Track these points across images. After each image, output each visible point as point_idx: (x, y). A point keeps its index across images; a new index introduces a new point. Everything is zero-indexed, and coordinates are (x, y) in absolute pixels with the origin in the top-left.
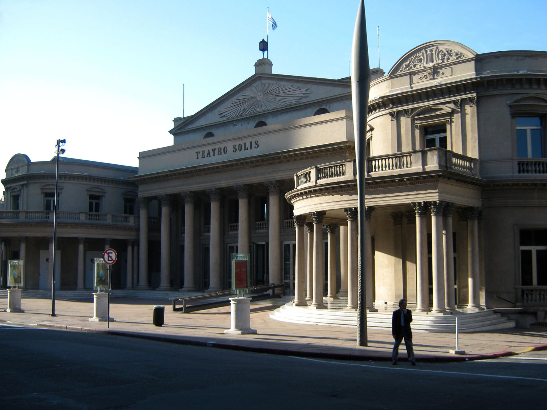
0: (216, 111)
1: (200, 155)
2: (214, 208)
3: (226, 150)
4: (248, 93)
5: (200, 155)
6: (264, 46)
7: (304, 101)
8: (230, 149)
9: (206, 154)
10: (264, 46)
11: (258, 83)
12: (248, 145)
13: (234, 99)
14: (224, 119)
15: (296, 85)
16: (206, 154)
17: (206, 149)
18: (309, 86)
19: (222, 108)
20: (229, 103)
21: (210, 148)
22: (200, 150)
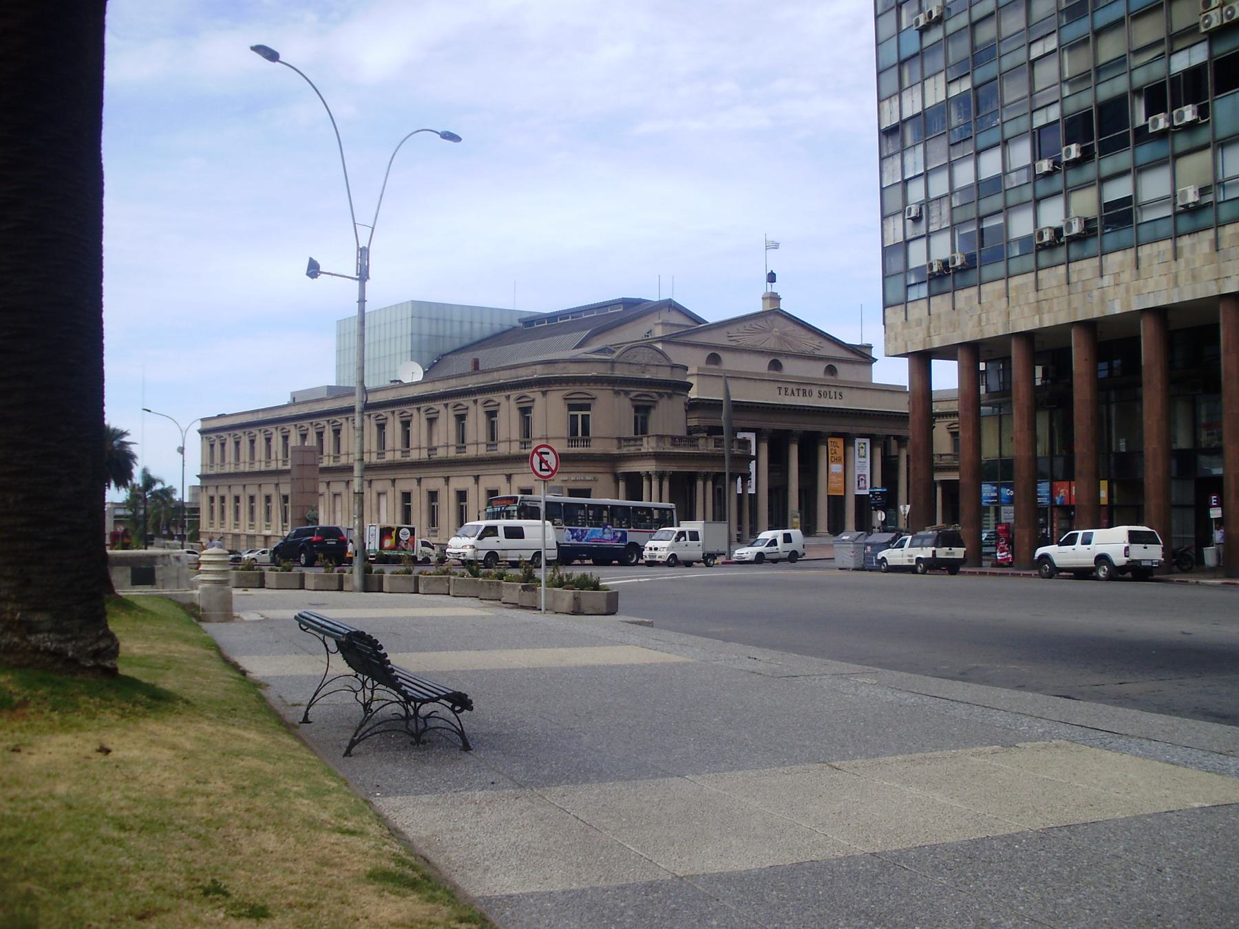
0: (725, 330)
1: (783, 391)
2: (794, 451)
3: (811, 393)
4: (762, 323)
5: (783, 391)
6: (772, 278)
7: (817, 353)
8: (815, 393)
9: (789, 392)
10: (772, 278)
11: (772, 317)
12: (833, 394)
13: (747, 324)
14: (734, 344)
15: (810, 335)
16: (789, 392)
17: (790, 387)
18: (821, 340)
19: (733, 330)
20: (740, 327)
21: (795, 387)
22: (783, 386)
